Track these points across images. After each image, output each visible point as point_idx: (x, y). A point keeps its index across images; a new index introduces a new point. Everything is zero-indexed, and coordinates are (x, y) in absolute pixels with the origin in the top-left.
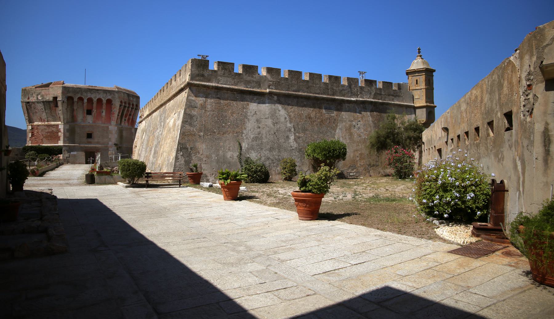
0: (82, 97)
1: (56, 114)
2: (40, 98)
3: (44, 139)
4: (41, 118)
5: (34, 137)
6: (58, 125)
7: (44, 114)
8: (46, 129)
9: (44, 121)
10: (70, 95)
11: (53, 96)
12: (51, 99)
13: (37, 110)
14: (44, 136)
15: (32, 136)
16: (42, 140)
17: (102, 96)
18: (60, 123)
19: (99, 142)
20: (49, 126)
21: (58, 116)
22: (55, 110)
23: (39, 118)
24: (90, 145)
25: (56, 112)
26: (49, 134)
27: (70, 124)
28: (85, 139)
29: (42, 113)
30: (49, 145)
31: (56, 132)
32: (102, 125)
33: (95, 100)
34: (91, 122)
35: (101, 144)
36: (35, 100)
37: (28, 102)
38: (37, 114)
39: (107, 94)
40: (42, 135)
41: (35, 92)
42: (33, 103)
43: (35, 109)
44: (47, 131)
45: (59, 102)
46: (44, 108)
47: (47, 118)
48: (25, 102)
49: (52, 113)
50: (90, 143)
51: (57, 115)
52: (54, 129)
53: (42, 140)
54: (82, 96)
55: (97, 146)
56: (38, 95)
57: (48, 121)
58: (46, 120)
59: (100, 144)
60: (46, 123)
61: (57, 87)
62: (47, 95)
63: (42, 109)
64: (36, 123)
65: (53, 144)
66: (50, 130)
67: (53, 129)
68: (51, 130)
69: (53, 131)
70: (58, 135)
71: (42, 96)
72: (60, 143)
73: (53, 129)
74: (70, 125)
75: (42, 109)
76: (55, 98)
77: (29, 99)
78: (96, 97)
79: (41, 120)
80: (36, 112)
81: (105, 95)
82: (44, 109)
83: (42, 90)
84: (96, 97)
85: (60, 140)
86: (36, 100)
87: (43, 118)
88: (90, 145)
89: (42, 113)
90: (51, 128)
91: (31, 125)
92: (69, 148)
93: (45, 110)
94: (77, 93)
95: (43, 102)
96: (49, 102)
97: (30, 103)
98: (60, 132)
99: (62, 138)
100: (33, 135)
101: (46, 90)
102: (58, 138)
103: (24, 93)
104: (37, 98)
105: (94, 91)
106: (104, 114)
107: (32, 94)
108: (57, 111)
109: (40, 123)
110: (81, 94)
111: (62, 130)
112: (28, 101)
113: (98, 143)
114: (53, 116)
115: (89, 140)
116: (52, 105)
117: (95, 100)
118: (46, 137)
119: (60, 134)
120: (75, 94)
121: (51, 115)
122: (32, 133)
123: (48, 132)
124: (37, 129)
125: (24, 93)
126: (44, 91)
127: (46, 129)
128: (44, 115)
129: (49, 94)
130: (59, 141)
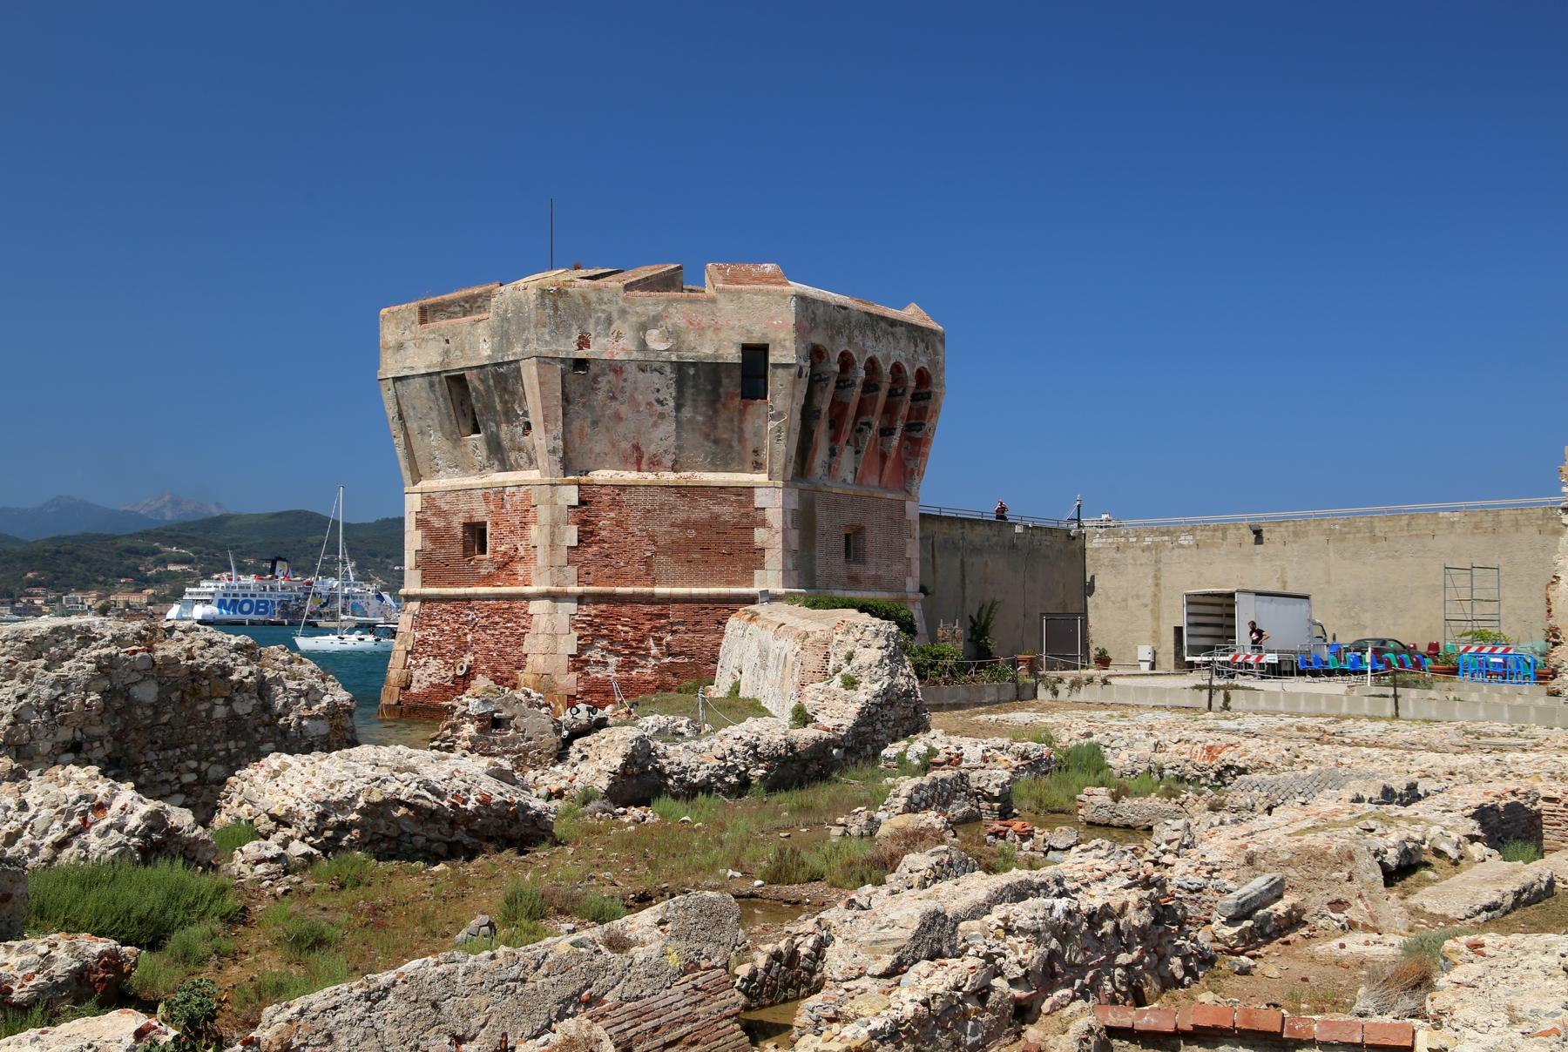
0: (851, 355)
1: (741, 430)
2: (662, 346)
3: (663, 558)
4: (637, 448)
5: (595, 548)
6: (749, 490)
7: (668, 427)
9: (655, 464)
10: (818, 338)
11: (744, 340)
12: (733, 355)
13: (624, 410)
15: (580, 541)
16: (647, 562)
18: (761, 478)
19: (880, 577)
20: (681, 490)
21: (750, 447)
22: (742, 412)
25: (741, 421)
26: (692, 533)
29: (651, 421)
31: (735, 526)
36: (629, 352)
37: (581, 364)
38: (621, 428)
39: (916, 346)
41: (623, 312)
42: (616, 368)
43: (613, 398)
44: (679, 517)
45: (780, 371)
47: (679, 448)
48: (563, 360)
49: (715, 427)
51: (741, 440)
52: (727, 512)
53: (647, 562)
54: (850, 350)
56: (644, 328)
57: (674, 470)
58: (668, 460)
59: (883, 589)
60: (669, 477)
61: (768, 293)
62: (701, 330)
63: (660, 402)
64: (601, 476)
65: (719, 584)
66: (700, 514)
67: (716, 509)
68: (706, 515)
70: (751, 542)
71: (674, 334)
72: (763, 582)
73: (716, 509)
75: (660, 402)
76: (755, 354)
77: (583, 342)
79: (637, 458)
80: (618, 417)
82: (672, 403)
83: (671, 302)
85: (761, 567)
86: (635, 355)
87: (650, 449)
89: (655, 425)
90: (703, 502)
91: (579, 485)
93: (678, 408)
95: (680, 367)
96: (713, 370)
97: (594, 369)
98: (763, 523)
99: (774, 559)
101: (694, 307)
102: (753, 558)
103: (556, 309)
104: (643, 346)
106: (895, 440)
107: (609, 321)
108: (749, 418)
109: (631, 476)
110: (850, 341)
111: (775, 516)
112: (581, 354)
114: (716, 442)
115: (856, 568)
116: (731, 385)
118: (677, 550)
119: (760, 535)
121: (707, 436)
122: (583, 523)
123: (685, 525)
125: (556, 309)
126: (685, 307)
128: (662, 436)
129: (717, 330)
130: (757, 573)
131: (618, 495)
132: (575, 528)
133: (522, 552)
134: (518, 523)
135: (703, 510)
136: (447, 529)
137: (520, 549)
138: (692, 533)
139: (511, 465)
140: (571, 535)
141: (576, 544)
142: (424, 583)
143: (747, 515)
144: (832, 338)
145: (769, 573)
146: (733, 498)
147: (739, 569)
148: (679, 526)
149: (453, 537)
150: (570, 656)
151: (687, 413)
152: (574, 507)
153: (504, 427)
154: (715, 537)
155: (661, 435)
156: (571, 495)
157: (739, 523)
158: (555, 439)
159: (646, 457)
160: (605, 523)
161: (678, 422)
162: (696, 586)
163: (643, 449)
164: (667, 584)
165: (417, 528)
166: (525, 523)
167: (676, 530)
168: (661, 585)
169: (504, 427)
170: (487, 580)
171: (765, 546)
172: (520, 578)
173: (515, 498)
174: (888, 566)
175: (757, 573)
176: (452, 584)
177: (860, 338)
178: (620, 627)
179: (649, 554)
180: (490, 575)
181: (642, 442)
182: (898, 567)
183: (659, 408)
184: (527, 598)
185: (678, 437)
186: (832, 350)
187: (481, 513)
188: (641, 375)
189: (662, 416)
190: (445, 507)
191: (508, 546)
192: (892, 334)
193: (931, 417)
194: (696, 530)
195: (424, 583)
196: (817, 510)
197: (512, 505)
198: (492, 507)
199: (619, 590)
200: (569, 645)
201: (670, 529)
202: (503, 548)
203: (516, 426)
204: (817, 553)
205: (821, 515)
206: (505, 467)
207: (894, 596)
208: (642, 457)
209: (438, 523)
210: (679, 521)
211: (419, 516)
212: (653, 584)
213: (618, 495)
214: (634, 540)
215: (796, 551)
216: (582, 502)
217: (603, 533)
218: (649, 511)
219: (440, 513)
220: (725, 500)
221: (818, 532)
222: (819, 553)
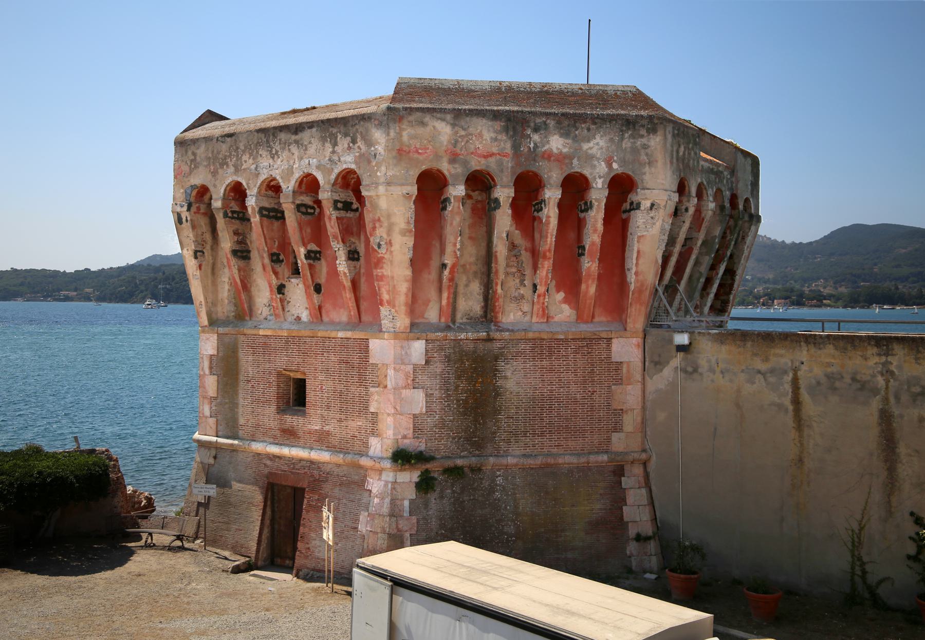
17: (314, 162)
19: (328, 433)
24: (286, 451)
27: (221, 330)
28: (269, 415)
32: (341, 334)
33: (288, 186)
34: (305, 316)
35: (331, 448)
39: (335, 144)
50: (289, 435)
55: (322, 456)
74: (219, 335)
78: (290, 171)
81: (329, 148)
84: (290, 171)
88: (286, 451)
92: (215, 458)
94: (222, 165)
105: (283, 136)
110: (237, 169)
113: (322, 439)
115: (291, 420)
117: (288, 186)
120: (214, 174)
144: (214, 174)
174: (340, 421)
177: (251, 161)
186: (215, 186)
192: (297, 142)
193: (374, 228)
196: (241, 355)
204: (241, 401)
205: (247, 363)
207: (339, 458)
215: (215, 398)
221: (241, 378)
222: (244, 400)
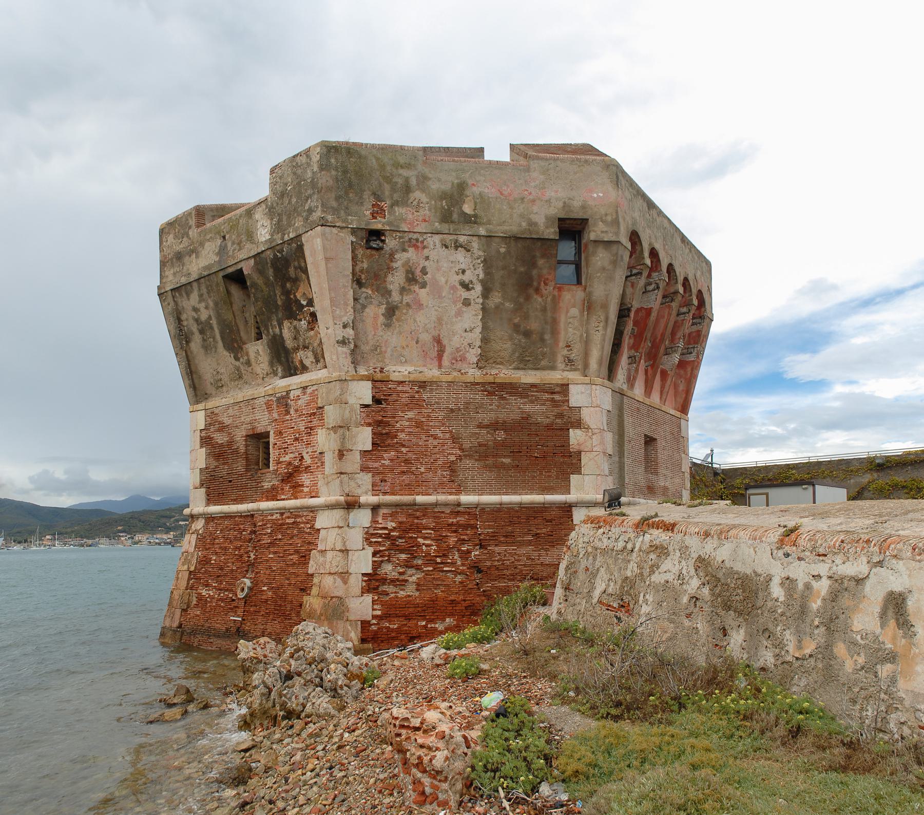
3: (468, 463)
4: (438, 341)
7: (472, 319)
8: (479, 407)
14: (467, 445)
16: (452, 468)
23: (426, 337)
26: (501, 435)
30: (506, 498)
31: (549, 427)
40: (455, 439)
44: (486, 417)
46: (483, 283)
51: (555, 332)
52: (539, 411)
53: (452, 468)
65: (531, 491)
69: (526, 418)
73: (528, 408)
82: (479, 288)
87: (452, 343)
89: (459, 314)
93: (486, 293)
98: (578, 424)
100: (382, 440)
121: (516, 328)
123: (494, 426)
124: (415, 403)
127: (479, 407)
130: (574, 478)
131: (417, 392)
132: (369, 430)
133: (308, 460)
134: (303, 428)
135: (516, 408)
136: (230, 443)
137: (306, 457)
138: (501, 435)
139: (296, 369)
140: (364, 438)
141: (370, 448)
142: (210, 501)
143: (560, 416)
145: (586, 478)
146: (547, 396)
147: (554, 473)
148: (487, 427)
149: (236, 451)
150: (364, 575)
151: (496, 298)
152: (367, 406)
153: (286, 324)
154: (526, 438)
155: (467, 326)
156: (363, 392)
157: (552, 424)
158: (345, 326)
159: (448, 350)
160: (404, 420)
161: (484, 309)
162: (507, 494)
163: (445, 342)
164: (474, 491)
165: (201, 447)
166: (311, 428)
167: (484, 431)
168: (467, 493)
169: (286, 324)
170: (272, 495)
171: (582, 448)
172: (306, 490)
173: (300, 402)
175: (574, 478)
176: (237, 501)
178: (421, 540)
179: (453, 458)
180: (274, 488)
181: (444, 334)
182: (677, 480)
183: (465, 294)
184: (313, 510)
185: (485, 328)
187: (263, 421)
188: (444, 252)
189: (467, 303)
190: (227, 421)
191: (292, 455)
194: (505, 431)
195: (210, 501)
197: (296, 411)
198: (276, 416)
199: (420, 499)
200: (362, 562)
201: (477, 431)
202: (287, 458)
203: (300, 320)
206: (291, 370)
208: (443, 351)
209: (220, 438)
210: (486, 422)
211: (203, 434)
212: (458, 492)
213: (417, 392)
214: (435, 442)
216: (377, 401)
217: (402, 436)
218: (452, 411)
219: (222, 428)
220: (537, 399)
221: (626, 438)
